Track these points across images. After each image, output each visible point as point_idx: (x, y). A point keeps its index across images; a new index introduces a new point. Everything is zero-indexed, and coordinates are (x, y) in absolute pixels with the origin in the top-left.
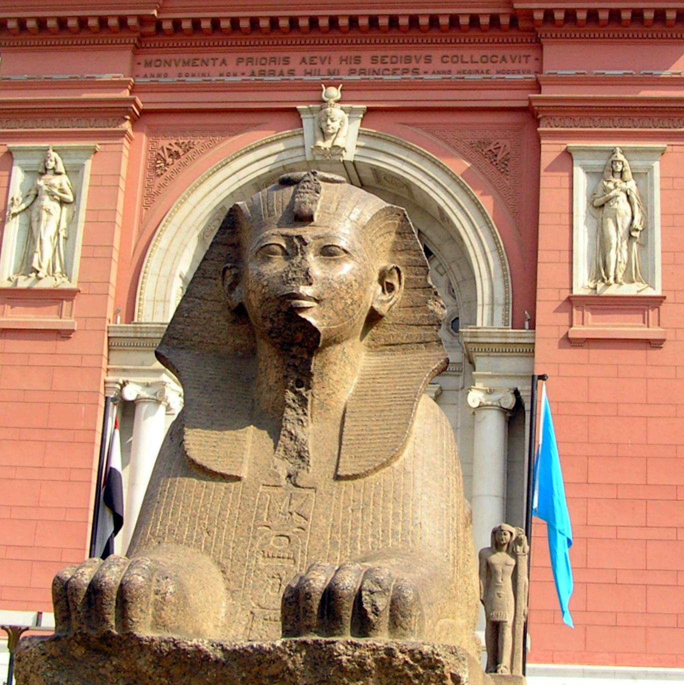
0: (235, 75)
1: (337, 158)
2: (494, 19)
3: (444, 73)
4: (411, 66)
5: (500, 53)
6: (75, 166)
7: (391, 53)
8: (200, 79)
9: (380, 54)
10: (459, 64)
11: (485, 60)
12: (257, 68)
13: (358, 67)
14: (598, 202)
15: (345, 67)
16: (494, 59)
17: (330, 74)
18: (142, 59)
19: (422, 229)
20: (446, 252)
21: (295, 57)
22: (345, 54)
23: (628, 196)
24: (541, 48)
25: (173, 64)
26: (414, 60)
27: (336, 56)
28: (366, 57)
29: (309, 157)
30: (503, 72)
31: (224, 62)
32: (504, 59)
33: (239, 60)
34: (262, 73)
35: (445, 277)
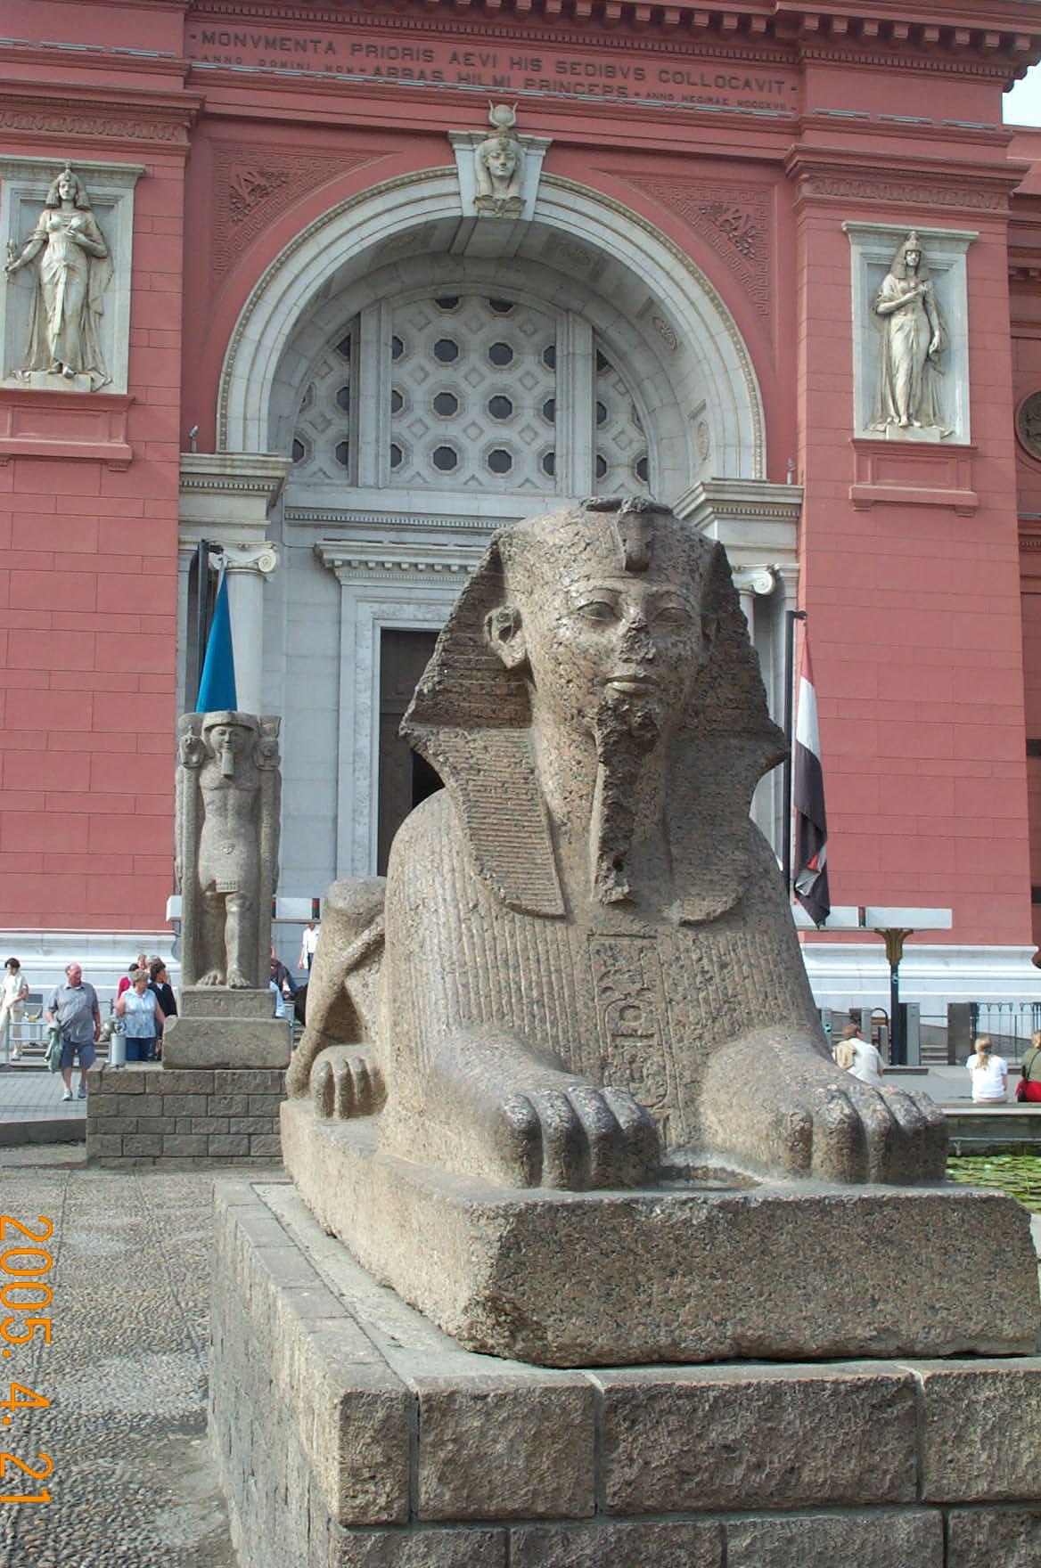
0: (350, 71)
1: (514, 216)
2: (745, 20)
3: (663, 97)
4: (617, 82)
5: (743, 74)
6: (106, 198)
7: (585, 59)
8: (298, 72)
9: (569, 58)
10: (685, 85)
11: (721, 81)
12: (385, 63)
13: (536, 76)
14: (882, 307)
15: (519, 75)
16: (734, 83)
17: (497, 83)
18: (199, 28)
19: (601, 323)
20: (641, 363)
21: (443, 50)
22: (518, 54)
23: (924, 302)
24: (800, 72)
25: (249, 43)
26: (619, 74)
27: (505, 54)
28: (549, 59)
29: (469, 211)
30: (754, 105)
31: (330, 47)
32: (747, 84)
33: (356, 48)
34: (392, 72)
35: (627, 400)
